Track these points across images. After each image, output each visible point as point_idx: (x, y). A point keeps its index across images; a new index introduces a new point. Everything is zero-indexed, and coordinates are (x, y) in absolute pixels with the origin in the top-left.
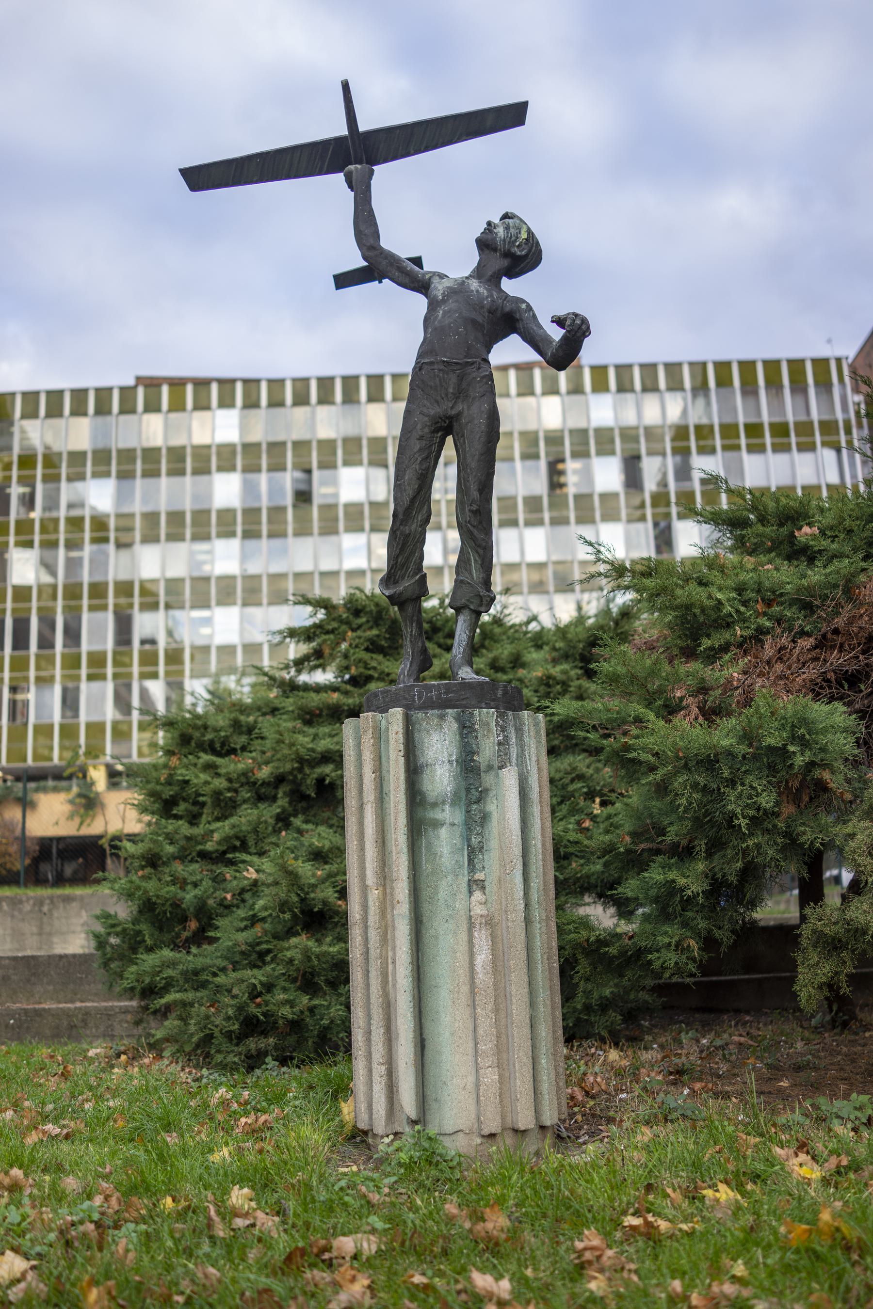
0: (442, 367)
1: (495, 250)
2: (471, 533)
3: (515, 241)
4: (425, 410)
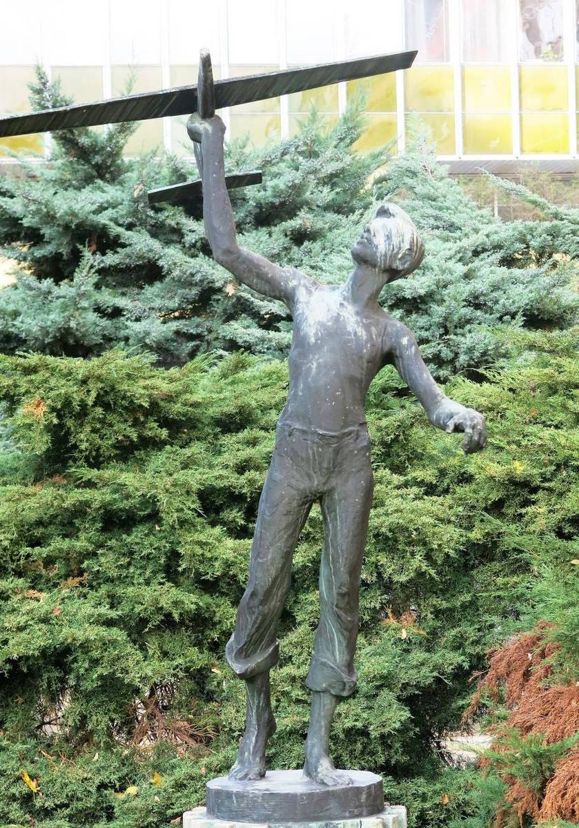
0: (317, 440)
1: (374, 266)
2: (339, 617)
3: (398, 253)
4: (293, 482)
